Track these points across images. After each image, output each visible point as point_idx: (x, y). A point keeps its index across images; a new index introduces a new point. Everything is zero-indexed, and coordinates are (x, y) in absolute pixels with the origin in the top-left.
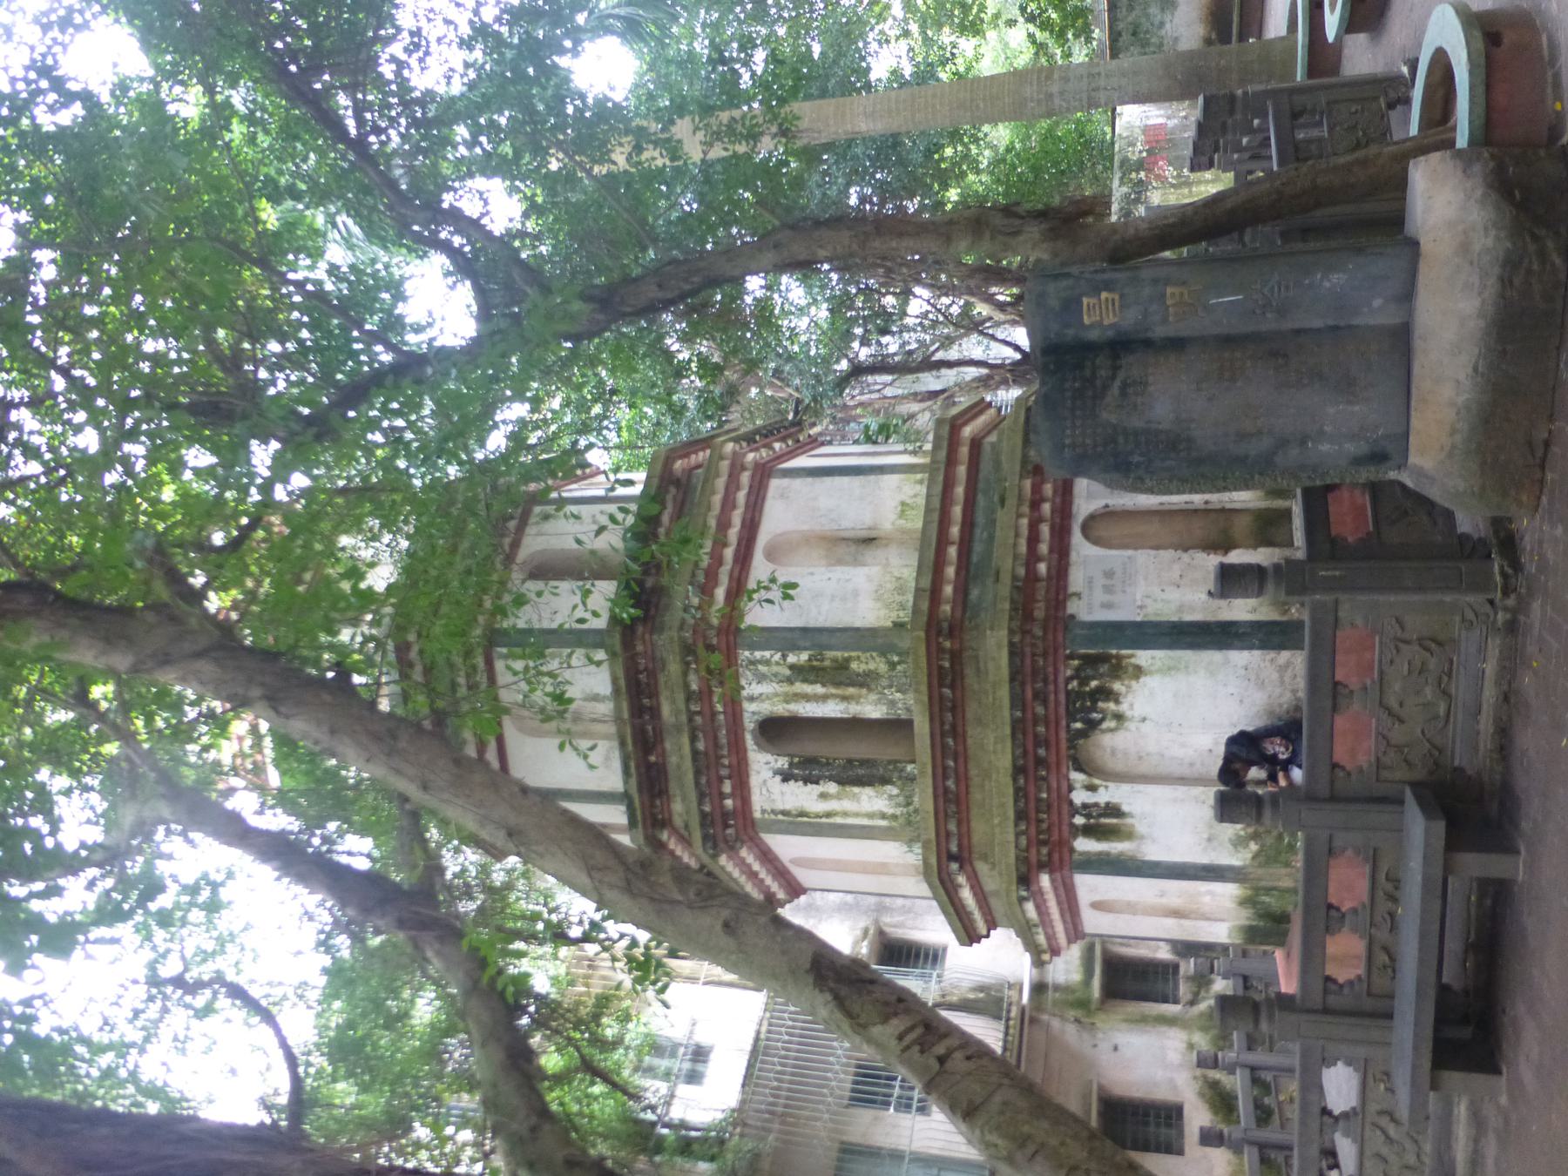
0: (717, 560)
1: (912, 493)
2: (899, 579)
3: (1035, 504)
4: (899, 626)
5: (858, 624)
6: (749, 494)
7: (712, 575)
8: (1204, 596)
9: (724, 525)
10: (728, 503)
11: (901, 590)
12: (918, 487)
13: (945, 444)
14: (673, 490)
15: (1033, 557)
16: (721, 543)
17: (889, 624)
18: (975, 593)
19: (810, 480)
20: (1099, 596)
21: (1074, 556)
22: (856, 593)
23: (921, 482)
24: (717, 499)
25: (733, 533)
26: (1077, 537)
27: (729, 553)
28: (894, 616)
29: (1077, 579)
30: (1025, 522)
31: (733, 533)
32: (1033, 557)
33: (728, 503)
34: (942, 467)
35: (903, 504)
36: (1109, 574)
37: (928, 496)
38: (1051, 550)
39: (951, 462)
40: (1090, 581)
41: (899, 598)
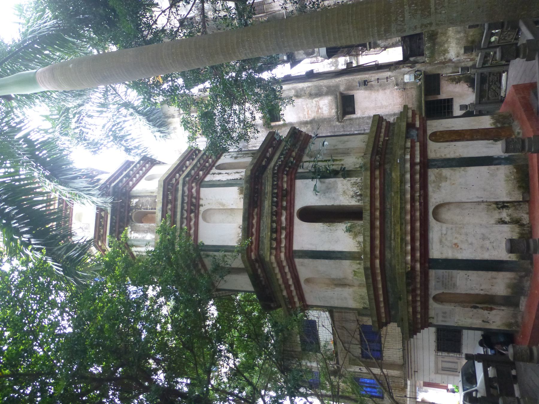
0: (290, 292)
1: (357, 267)
2: (361, 295)
3: (414, 301)
4: (364, 308)
5: (350, 307)
6: (289, 268)
7: (291, 297)
8: (480, 322)
9: (286, 281)
10: (284, 275)
11: (362, 298)
12: (359, 266)
13: (370, 277)
14: (257, 265)
15: (415, 312)
16: (288, 287)
17: (361, 307)
18: (393, 313)
19: (311, 260)
20: (440, 318)
21: (430, 307)
22: (346, 298)
23: (360, 264)
24: (279, 276)
25: (291, 282)
26: (431, 301)
27: (293, 288)
28: (362, 306)
29: (432, 313)
30: (411, 310)
31: (291, 282)
32: (415, 312)
33: (284, 275)
34: (371, 285)
35: (354, 271)
36: (445, 313)
37: (369, 295)
38: (421, 309)
39: (374, 281)
40: (437, 314)
41: (363, 301)
